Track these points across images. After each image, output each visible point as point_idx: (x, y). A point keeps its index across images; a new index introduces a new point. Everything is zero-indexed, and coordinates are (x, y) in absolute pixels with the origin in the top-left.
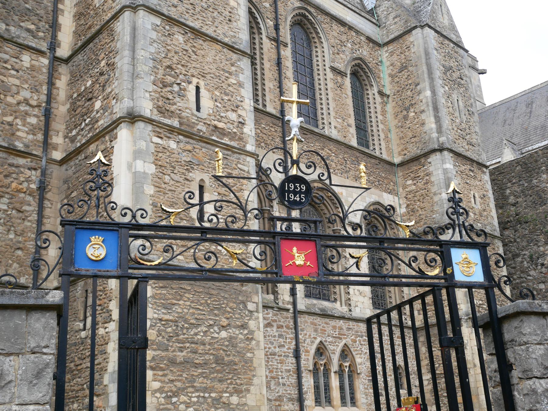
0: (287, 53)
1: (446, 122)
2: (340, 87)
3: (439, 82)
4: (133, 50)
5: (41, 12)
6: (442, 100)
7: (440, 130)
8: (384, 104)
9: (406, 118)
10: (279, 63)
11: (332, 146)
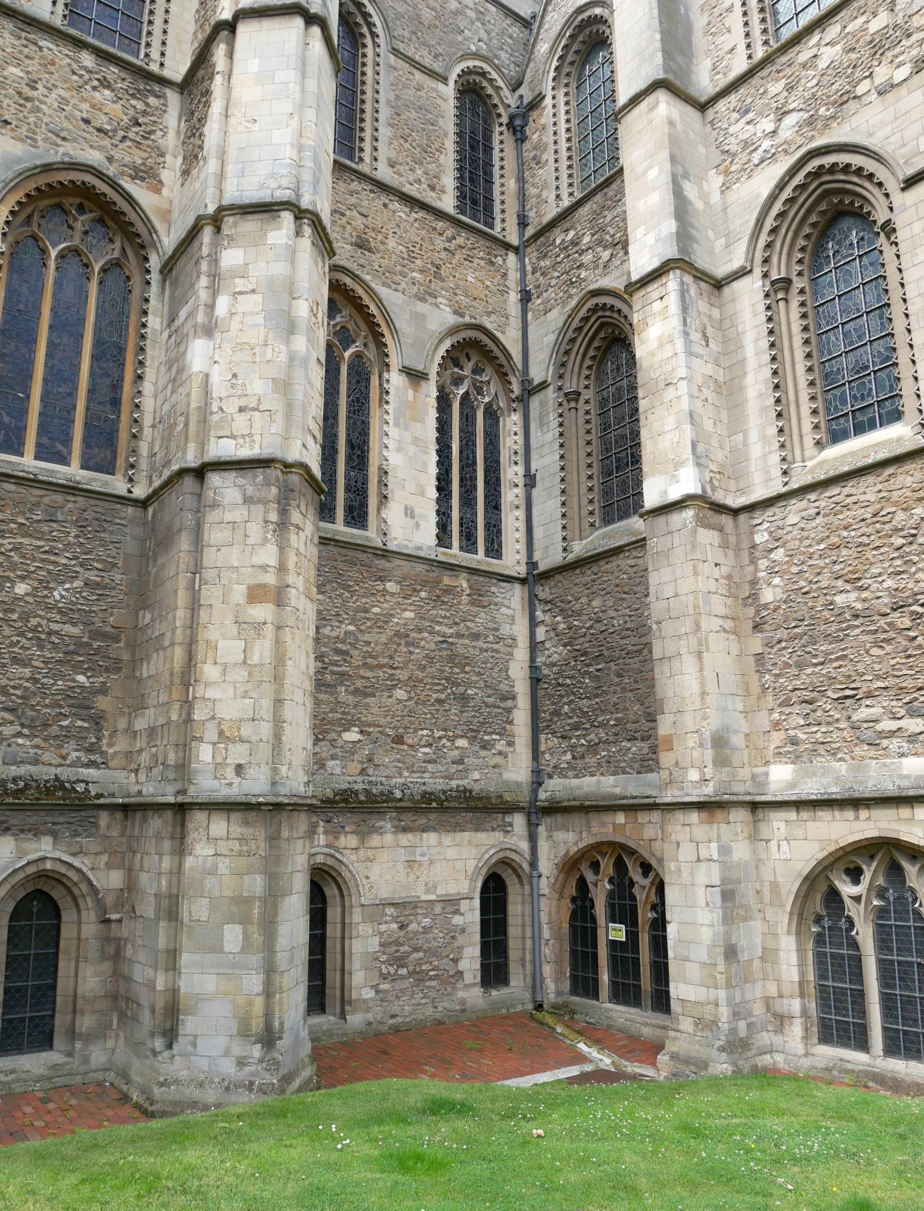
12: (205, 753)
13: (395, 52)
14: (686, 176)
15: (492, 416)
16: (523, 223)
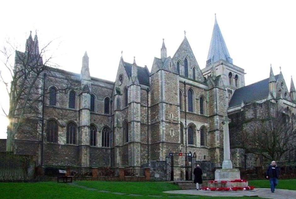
0: (187, 98)
1: (218, 109)
2: (198, 102)
3: (218, 100)
4: (162, 109)
5: (145, 99)
6: (218, 104)
7: (217, 111)
8: (207, 104)
9: (211, 107)
10: (185, 101)
11: (195, 115)
12: (82, 164)
13: (98, 99)
14: (118, 118)
15: (108, 133)
16: (111, 114)
